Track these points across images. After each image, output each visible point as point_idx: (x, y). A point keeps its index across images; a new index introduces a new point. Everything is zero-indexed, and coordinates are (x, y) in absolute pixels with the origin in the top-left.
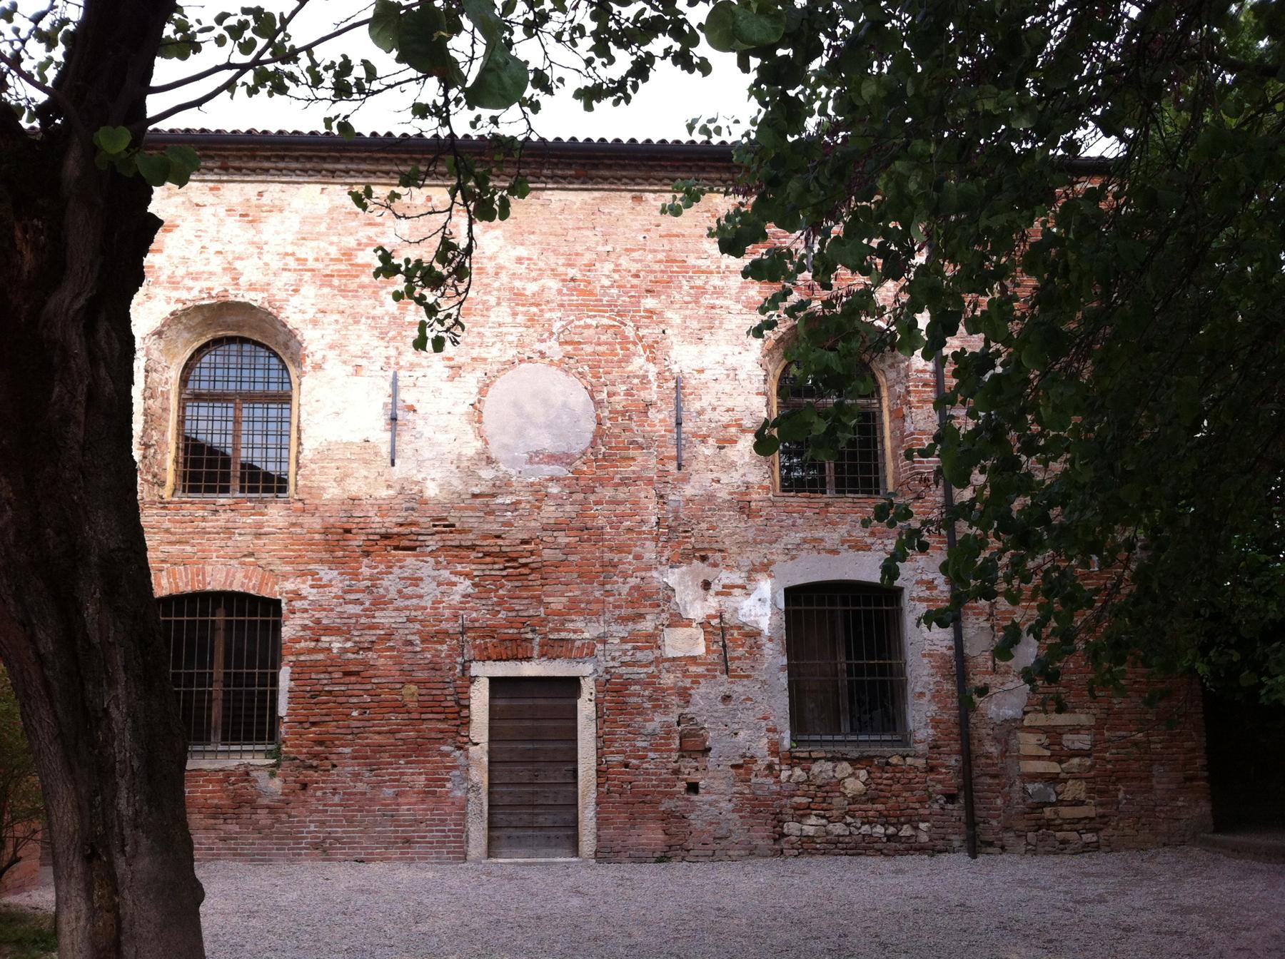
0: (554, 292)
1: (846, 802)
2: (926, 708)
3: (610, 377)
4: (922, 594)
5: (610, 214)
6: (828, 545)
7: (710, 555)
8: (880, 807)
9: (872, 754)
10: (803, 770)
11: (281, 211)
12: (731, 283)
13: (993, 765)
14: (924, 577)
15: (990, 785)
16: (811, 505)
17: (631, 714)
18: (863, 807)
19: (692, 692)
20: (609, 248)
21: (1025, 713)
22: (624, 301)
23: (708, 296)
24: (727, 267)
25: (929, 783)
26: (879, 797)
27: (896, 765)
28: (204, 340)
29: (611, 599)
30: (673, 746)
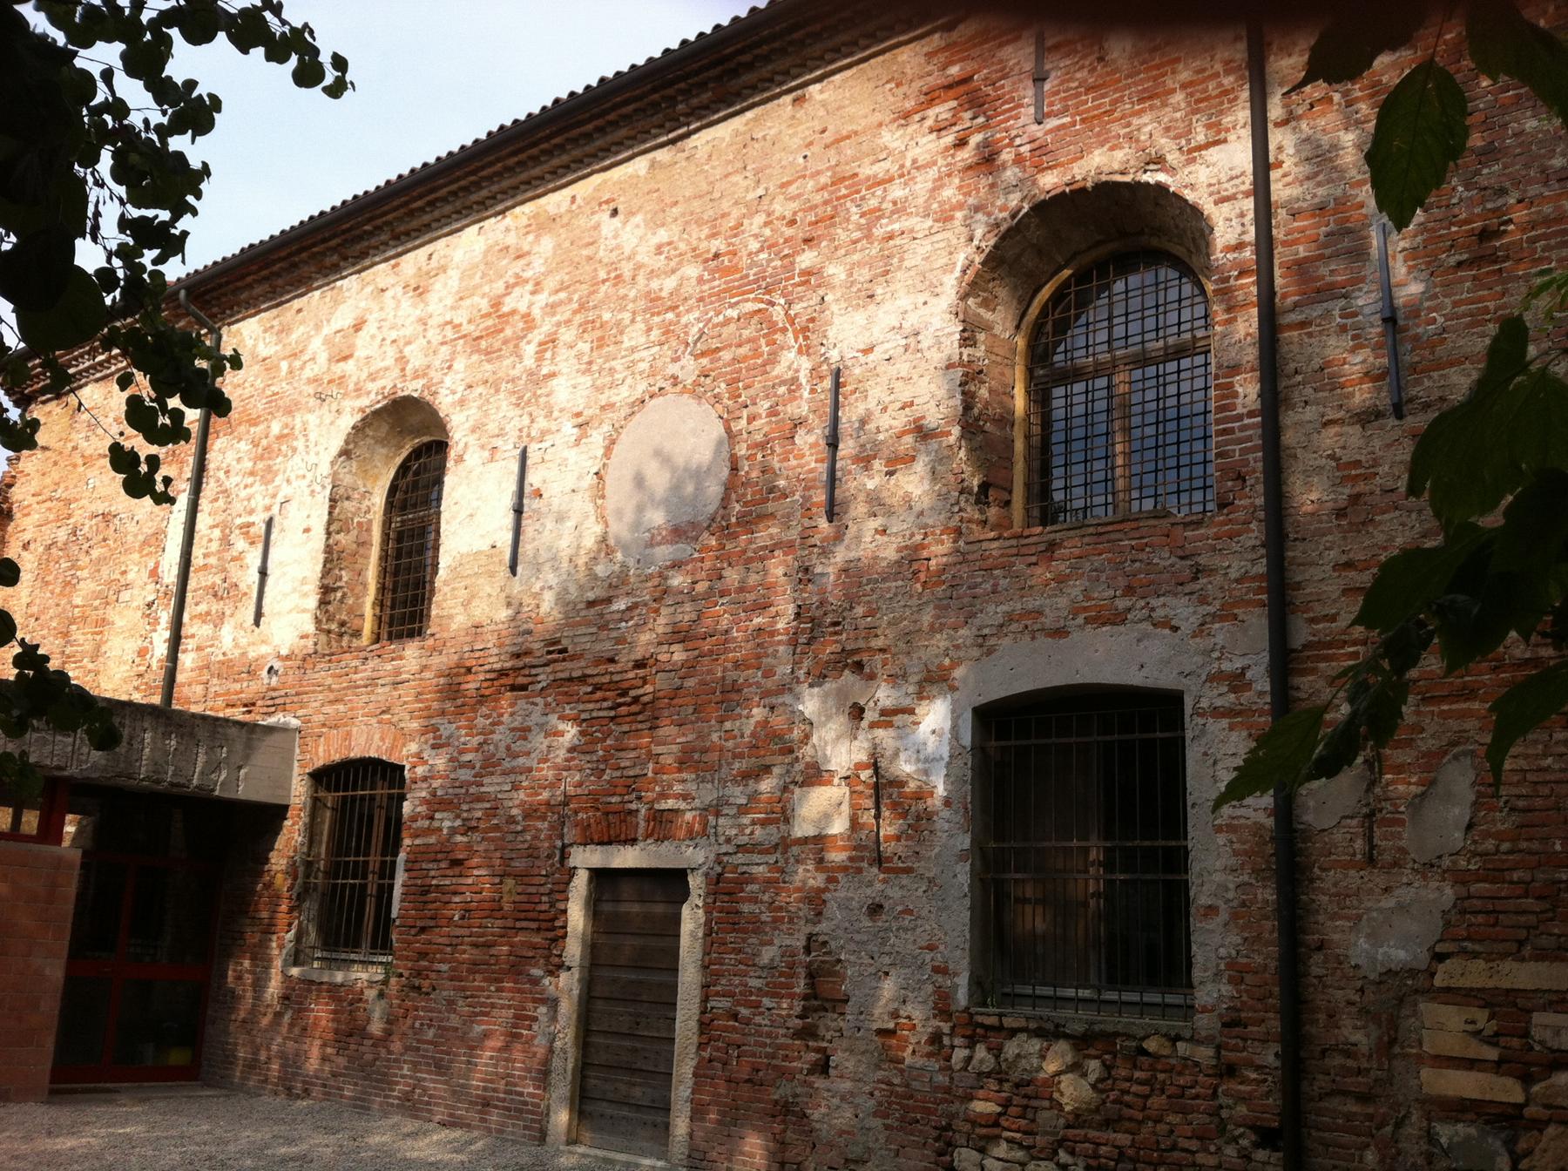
0: (694, 282)
1: (1062, 1121)
2: (1217, 939)
3: (752, 392)
4: (1219, 702)
5: (764, 138)
6: (1048, 621)
7: (865, 659)
8: (1123, 1139)
9: (1110, 1028)
10: (989, 1050)
11: (445, 271)
12: (919, 186)
13: (1359, 1072)
14: (1226, 666)
15: (1349, 1117)
16: (1024, 550)
17: (745, 931)
18: (1092, 1134)
19: (827, 896)
20: (760, 192)
21: (1440, 958)
22: (775, 268)
23: (884, 221)
24: (914, 161)
25: (1223, 1100)
26: (1121, 1118)
27: (1156, 1057)
28: (405, 453)
29: (730, 744)
30: (797, 990)
